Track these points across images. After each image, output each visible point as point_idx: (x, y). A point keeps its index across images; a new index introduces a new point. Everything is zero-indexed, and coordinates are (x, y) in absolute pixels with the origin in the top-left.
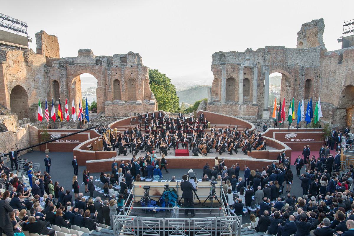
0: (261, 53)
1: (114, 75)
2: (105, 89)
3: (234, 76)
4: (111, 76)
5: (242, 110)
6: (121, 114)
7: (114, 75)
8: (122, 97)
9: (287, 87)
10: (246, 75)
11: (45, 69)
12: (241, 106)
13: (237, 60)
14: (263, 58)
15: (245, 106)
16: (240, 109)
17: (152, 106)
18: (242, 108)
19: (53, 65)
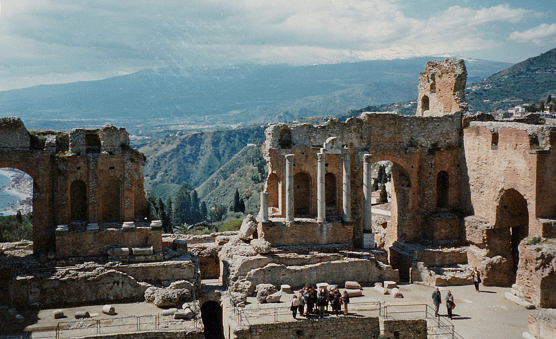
3: (307, 168)
5: (325, 233)
9: (403, 186)
10: (329, 166)
12: (322, 226)
14: (359, 135)
15: (330, 225)
16: (321, 230)
18: (325, 229)
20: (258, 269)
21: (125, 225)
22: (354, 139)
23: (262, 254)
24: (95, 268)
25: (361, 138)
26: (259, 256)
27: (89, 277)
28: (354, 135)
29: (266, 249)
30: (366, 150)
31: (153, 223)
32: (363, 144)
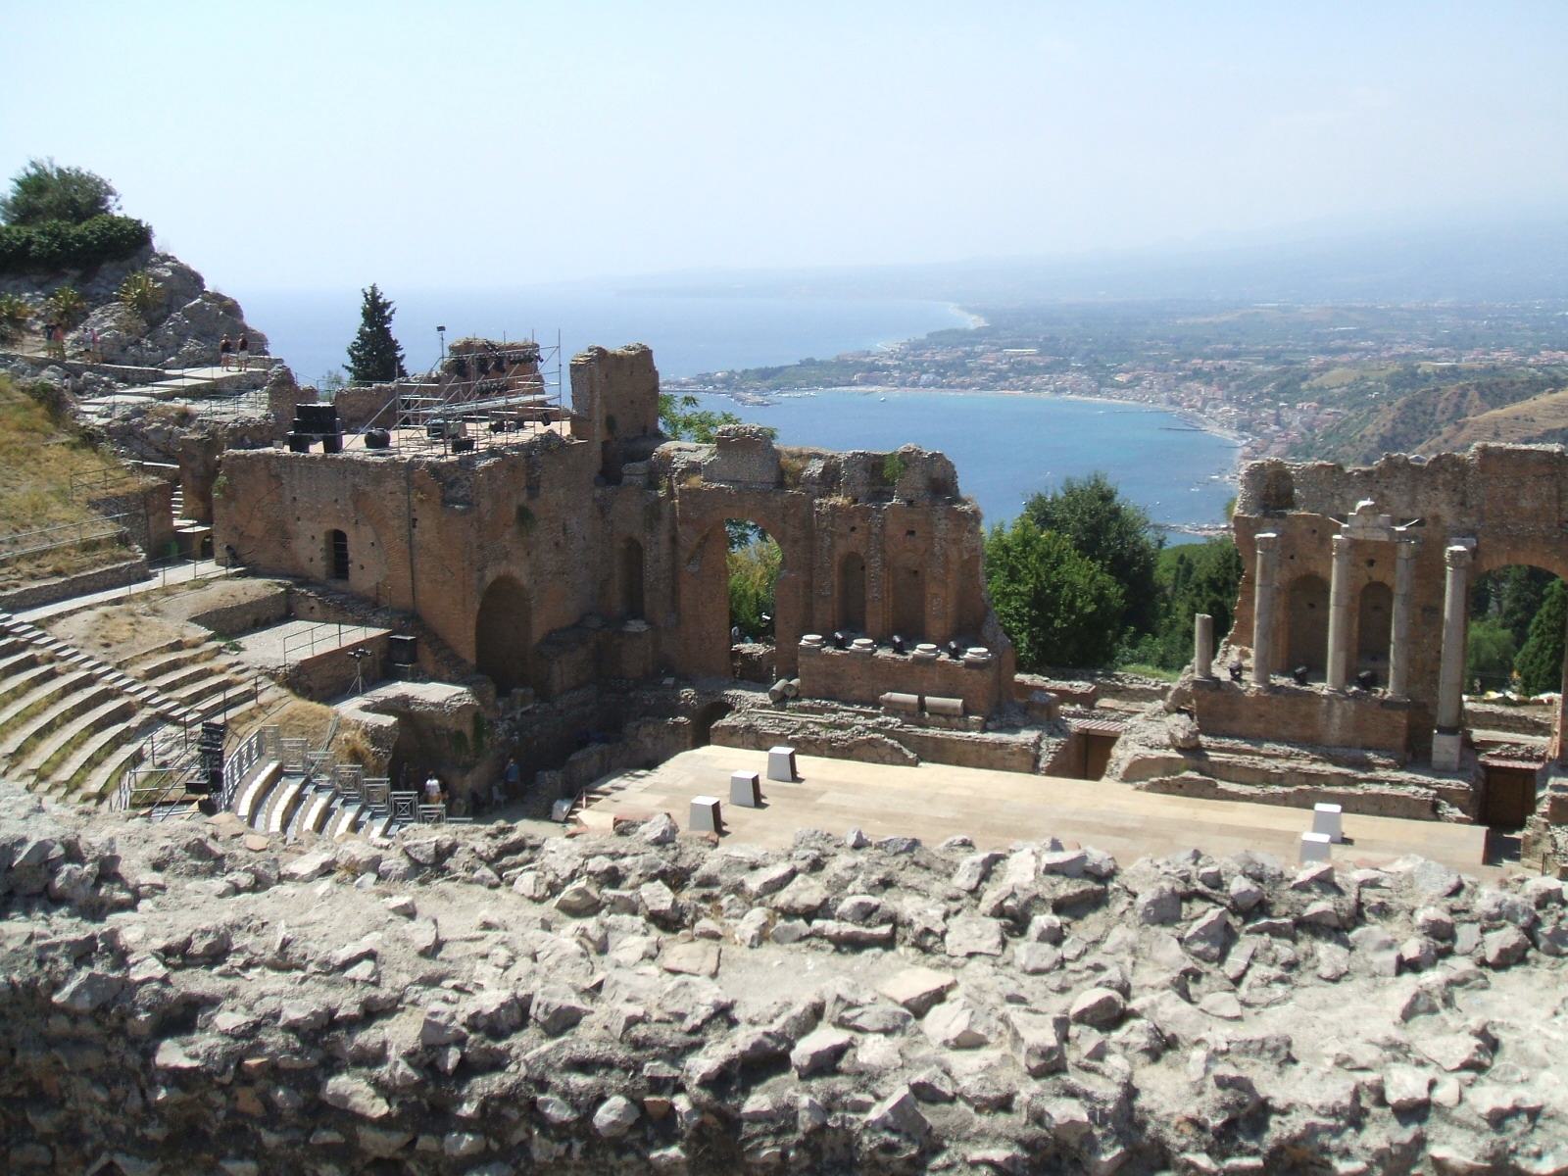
0: (1449, 477)
1: (841, 536)
2: (809, 585)
4: (832, 534)
5: (1337, 721)
6: (856, 692)
7: (841, 536)
8: (872, 622)
11: (598, 492)
12: (1330, 704)
13: (1337, 502)
14: (1457, 498)
16: (1328, 712)
17: (975, 672)
18: (1337, 711)
19: (626, 479)
20: (1155, 780)
21: (922, 649)
22: (1443, 506)
23: (1179, 750)
24: (851, 725)
25: (1462, 504)
26: (1172, 753)
27: (837, 740)
28: (1442, 496)
29: (1183, 740)
30: (1461, 535)
31: (973, 653)
32: (1465, 519)
